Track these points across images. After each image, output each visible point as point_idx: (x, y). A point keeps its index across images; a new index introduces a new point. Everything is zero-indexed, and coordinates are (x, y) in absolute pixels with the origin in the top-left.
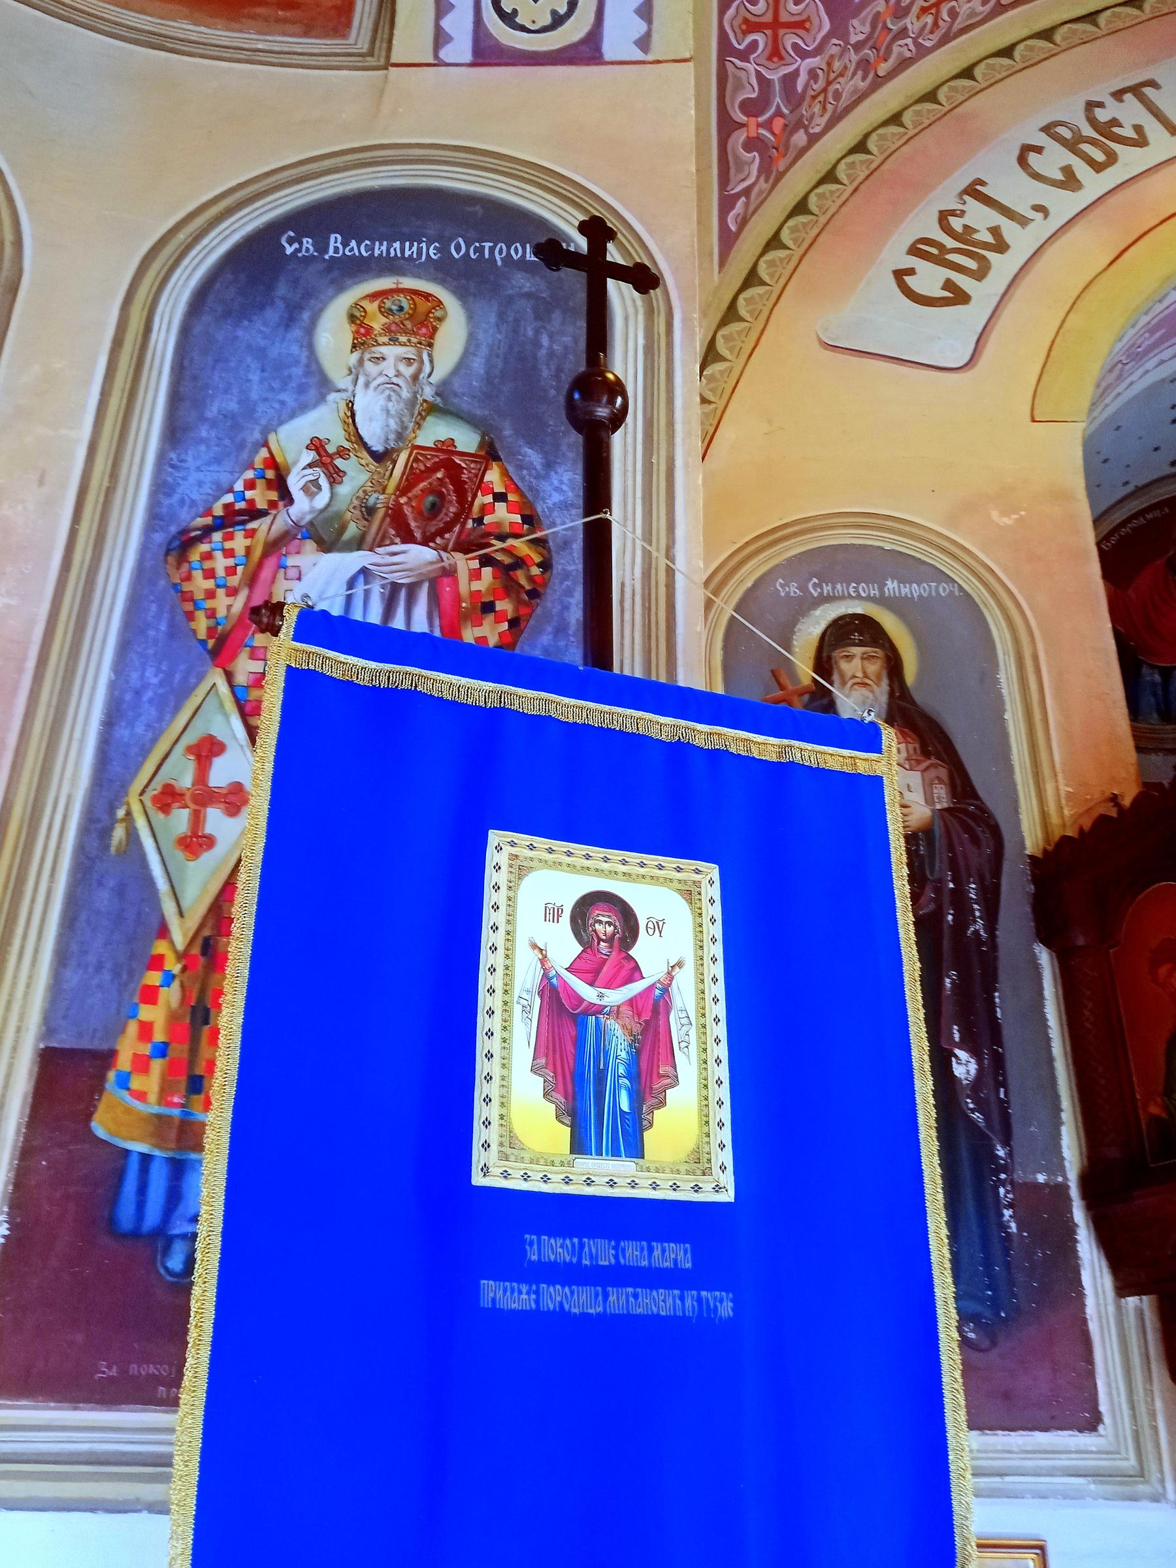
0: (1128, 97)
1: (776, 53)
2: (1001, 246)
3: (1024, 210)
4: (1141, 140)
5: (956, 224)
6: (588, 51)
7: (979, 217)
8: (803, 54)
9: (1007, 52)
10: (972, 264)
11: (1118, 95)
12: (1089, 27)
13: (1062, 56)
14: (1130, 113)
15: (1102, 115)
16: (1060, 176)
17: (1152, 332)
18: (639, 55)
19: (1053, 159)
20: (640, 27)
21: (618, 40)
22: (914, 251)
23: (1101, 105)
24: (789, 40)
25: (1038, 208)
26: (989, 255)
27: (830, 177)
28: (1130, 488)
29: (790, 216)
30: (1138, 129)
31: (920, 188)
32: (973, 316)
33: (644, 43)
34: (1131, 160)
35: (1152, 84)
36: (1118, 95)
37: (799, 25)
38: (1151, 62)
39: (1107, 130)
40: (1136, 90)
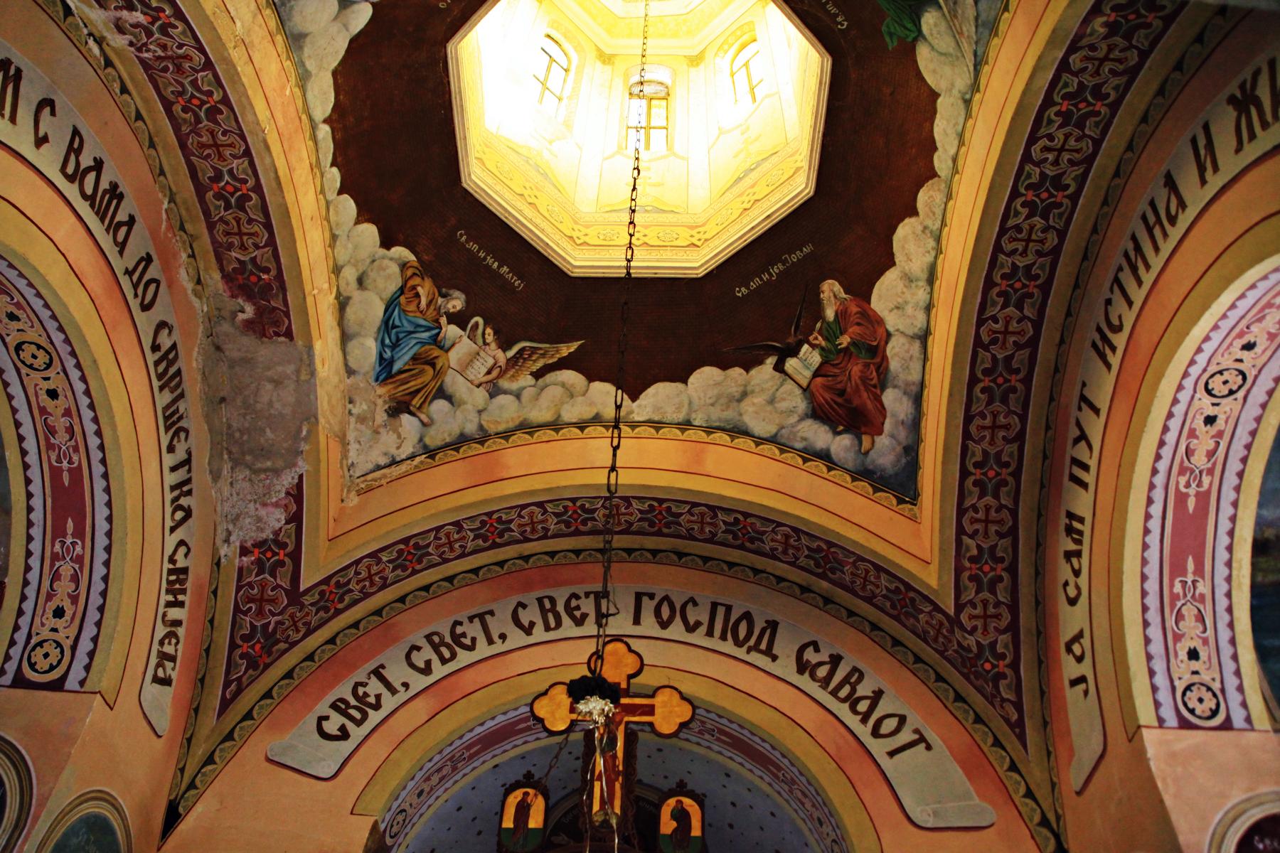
0: (476, 620)
1: (260, 613)
2: (377, 707)
3: (397, 685)
4: (471, 648)
5: (361, 691)
6: (57, 686)
7: (375, 687)
8: (274, 615)
9: (426, 588)
10: (357, 715)
11: (471, 619)
12: (474, 577)
13: (455, 593)
14: (474, 630)
15: (459, 630)
16: (422, 665)
17: (468, 748)
18: (77, 688)
19: (428, 653)
20: (83, 674)
21: (71, 683)
22: (334, 706)
23: (461, 624)
24: (268, 607)
25: (406, 685)
26: (370, 712)
27: (310, 657)
28: (567, 791)
29: (282, 679)
30: (474, 640)
31: (353, 667)
32: (346, 747)
33: (82, 683)
34: (464, 657)
35: (491, 613)
36: (471, 619)
37: (273, 601)
38: (495, 600)
39: (457, 638)
40: (481, 616)
